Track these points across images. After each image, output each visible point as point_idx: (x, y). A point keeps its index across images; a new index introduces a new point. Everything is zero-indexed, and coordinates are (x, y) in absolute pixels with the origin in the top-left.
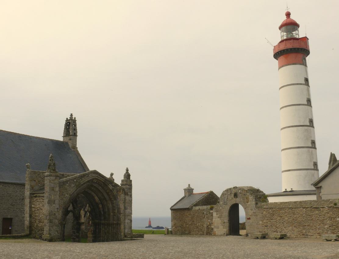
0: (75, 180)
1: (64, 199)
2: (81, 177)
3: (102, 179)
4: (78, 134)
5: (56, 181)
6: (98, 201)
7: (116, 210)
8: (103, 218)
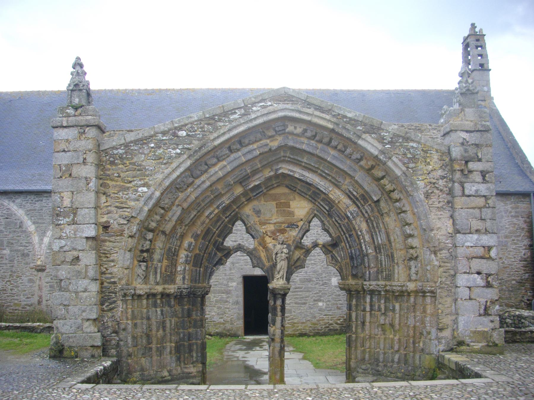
0: (183, 133)
2: (212, 118)
4: (491, 65)
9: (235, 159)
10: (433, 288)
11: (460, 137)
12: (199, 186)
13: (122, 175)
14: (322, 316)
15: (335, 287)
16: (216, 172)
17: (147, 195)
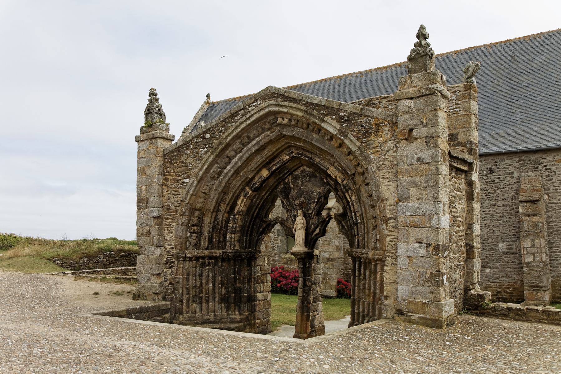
0: (208, 136)
2: (224, 121)
9: (248, 151)
10: (381, 257)
11: (405, 105)
12: (227, 174)
13: (176, 171)
14: (489, 283)
15: (504, 253)
16: (237, 163)
17: (189, 185)
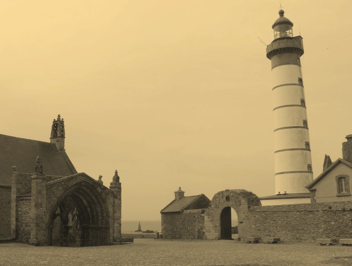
0: (63, 183)
1: (51, 202)
2: (69, 179)
3: (90, 182)
4: (66, 136)
5: (44, 184)
6: (87, 204)
7: (105, 214)
8: (91, 222)
